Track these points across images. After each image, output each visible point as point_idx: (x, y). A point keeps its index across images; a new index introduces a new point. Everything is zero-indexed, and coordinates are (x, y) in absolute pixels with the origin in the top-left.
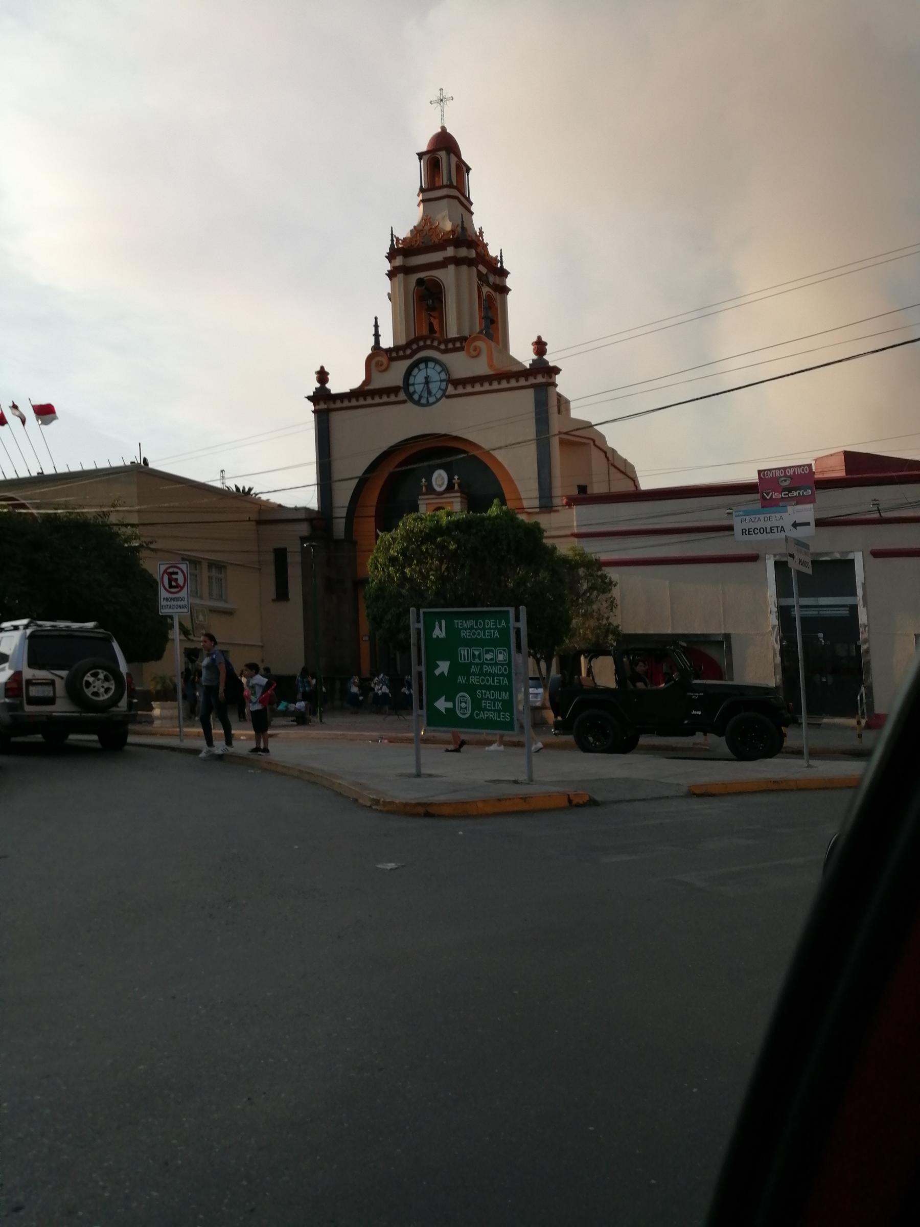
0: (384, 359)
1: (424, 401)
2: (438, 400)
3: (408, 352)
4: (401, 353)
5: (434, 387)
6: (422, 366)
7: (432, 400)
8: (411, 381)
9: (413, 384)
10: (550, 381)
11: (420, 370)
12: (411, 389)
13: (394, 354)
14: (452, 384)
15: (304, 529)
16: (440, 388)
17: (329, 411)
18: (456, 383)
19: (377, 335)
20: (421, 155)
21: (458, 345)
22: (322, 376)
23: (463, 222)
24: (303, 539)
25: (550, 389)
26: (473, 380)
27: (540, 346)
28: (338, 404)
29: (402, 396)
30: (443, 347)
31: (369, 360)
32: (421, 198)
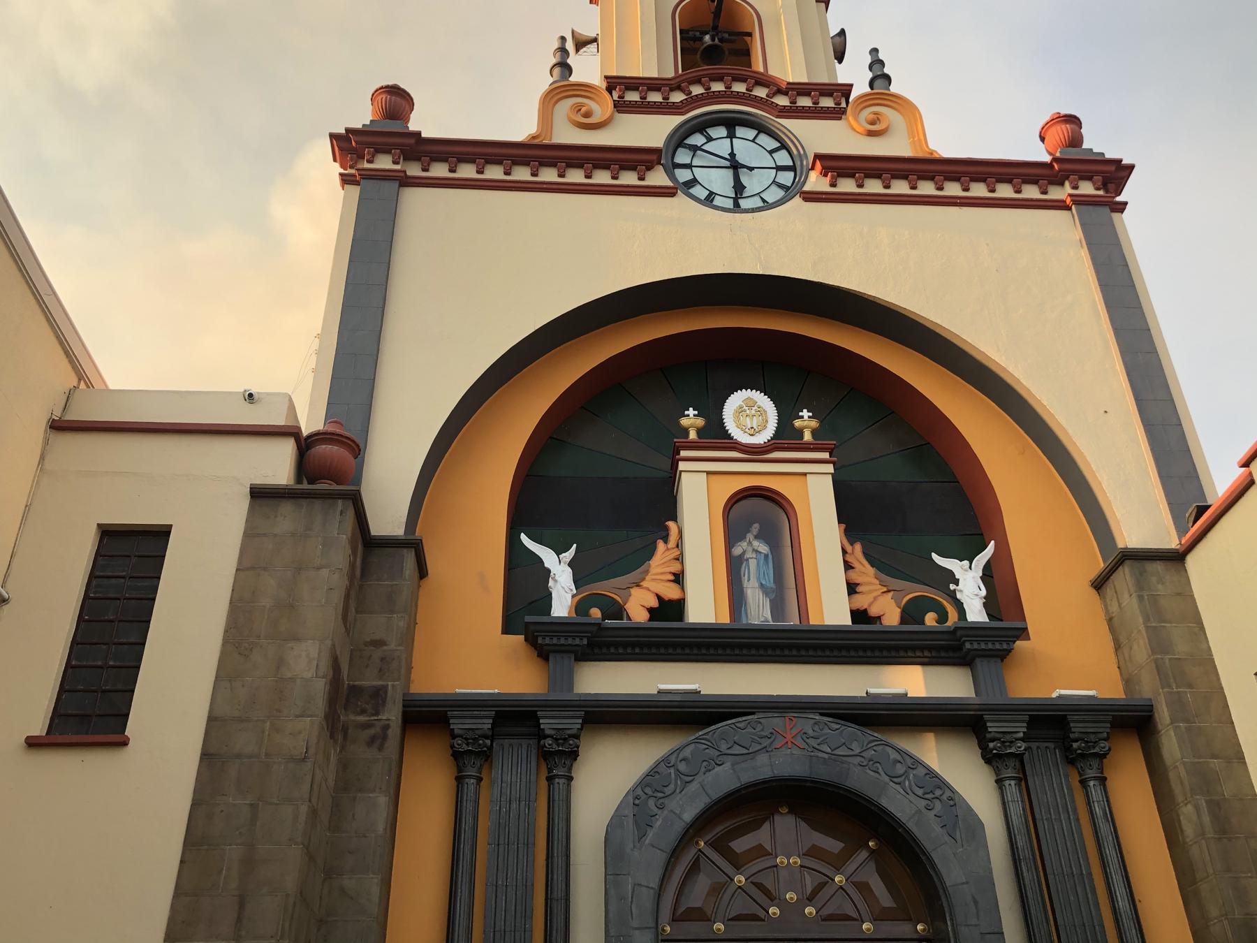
1: (718, 201)
4: (655, 97)
5: (753, 183)
6: (721, 132)
7: (744, 204)
8: (682, 157)
9: (689, 166)
11: (710, 139)
13: (633, 96)
15: (277, 465)
17: (407, 182)
19: (564, 67)
21: (827, 102)
24: (261, 495)
25: (1115, 216)
28: (440, 170)
29: (658, 178)
30: (782, 101)
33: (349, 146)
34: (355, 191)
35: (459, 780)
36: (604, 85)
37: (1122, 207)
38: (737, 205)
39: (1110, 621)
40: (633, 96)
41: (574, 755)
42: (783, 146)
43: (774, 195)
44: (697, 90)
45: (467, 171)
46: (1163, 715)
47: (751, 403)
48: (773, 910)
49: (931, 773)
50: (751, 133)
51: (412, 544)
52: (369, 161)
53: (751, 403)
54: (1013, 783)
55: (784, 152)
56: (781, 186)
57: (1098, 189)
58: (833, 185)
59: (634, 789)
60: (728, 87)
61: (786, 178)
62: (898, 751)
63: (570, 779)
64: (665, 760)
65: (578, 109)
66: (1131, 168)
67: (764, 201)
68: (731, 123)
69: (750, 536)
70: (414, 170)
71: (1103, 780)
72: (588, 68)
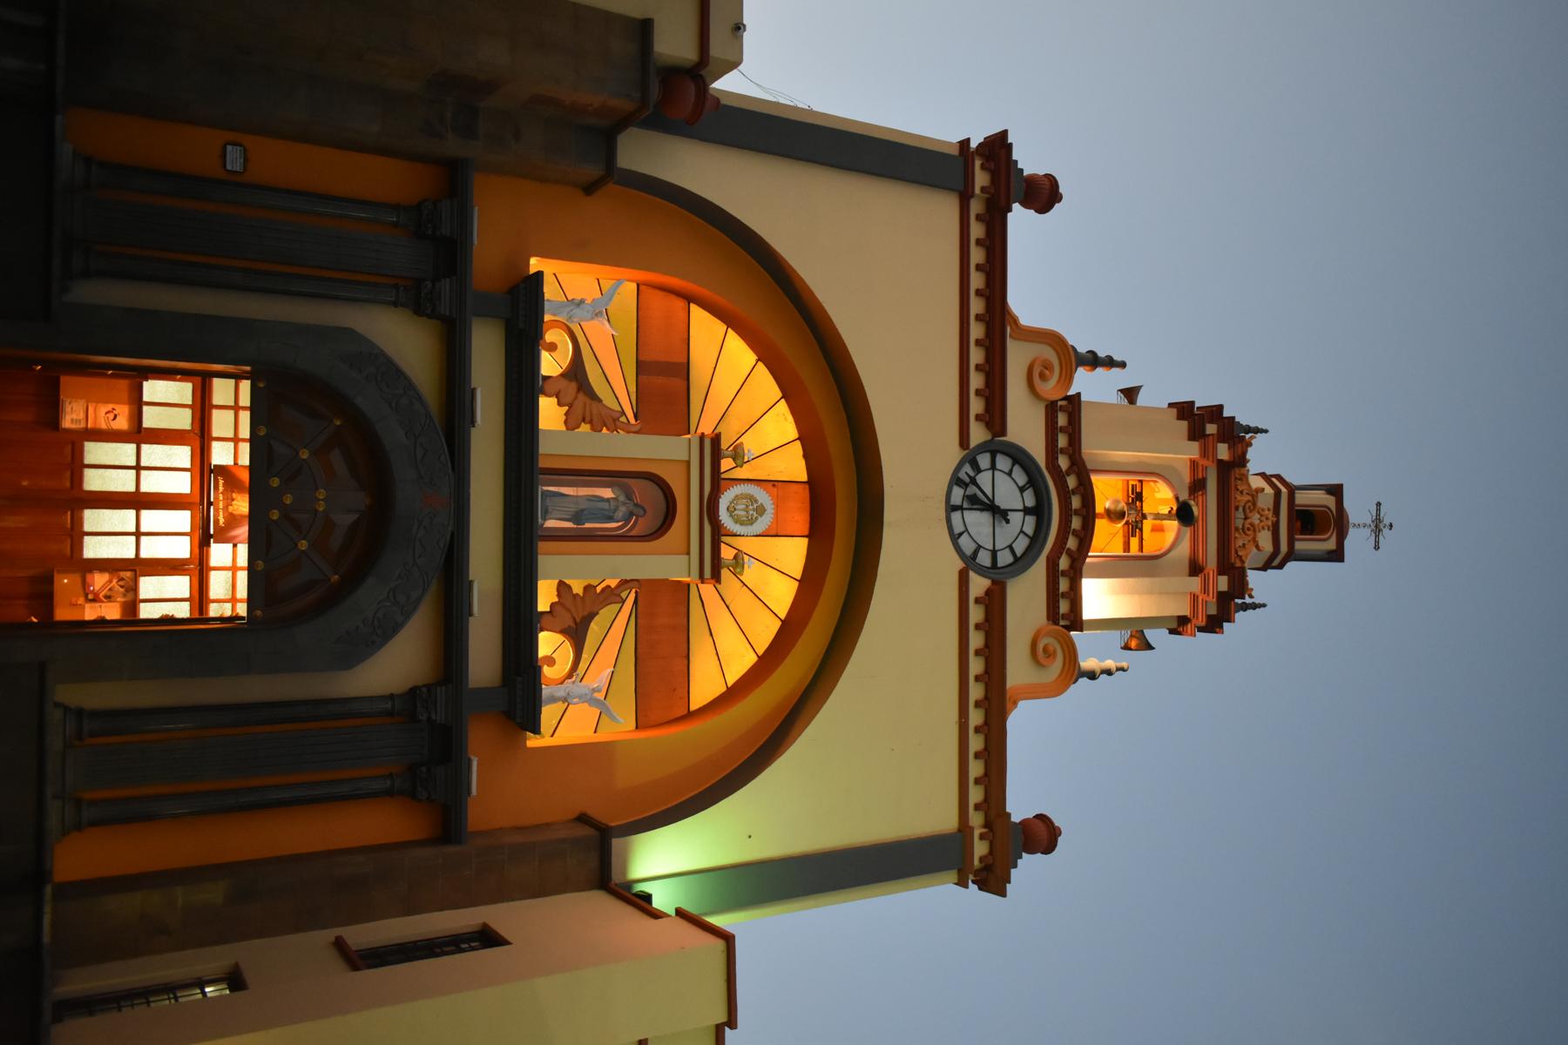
0: (1050, 389)
2: (955, 538)
3: (1063, 462)
4: (1062, 441)
6: (1030, 501)
8: (1003, 462)
9: (993, 467)
10: (971, 877)
11: (1022, 490)
12: (984, 460)
13: (1062, 420)
14: (988, 592)
15: (674, 44)
16: (980, 547)
17: (965, 198)
18: (995, 603)
19: (1093, 361)
20: (1336, 491)
22: (1043, 194)
23: (1255, 606)
24: (644, 29)
26: (995, 651)
27: (1041, 835)
28: (977, 231)
29: (978, 434)
30: (1064, 563)
31: (1054, 340)
32: (1284, 490)
33: (998, 148)
34: (955, 152)
35: (396, 208)
36: (1071, 392)
37: (962, 883)
38: (955, 508)
39: (548, 825)
40: (1062, 420)
41: (418, 311)
42: (1016, 559)
43: (967, 545)
44: (1072, 482)
45: (977, 255)
46: (449, 849)
47: (761, 510)
48: (275, 482)
49: (396, 628)
50: (1029, 529)
51: (607, 176)
52: (983, 167)
53: (761, 510)
54: (389, 706)
55: (1010, 559)
56: (976, 553)
57: (981, 859)
58: (977, 601)
59: (383, 354)
60: (1077, 512)
61: (984, 559)
62: (419, 600)
63: (395, 304)
64: (409, 385)
65: (1047, 366)
66: (1003, 893)
67: (961, 534)
68: (1039, 511)
69: (632, 508)
70: (976, 207)
71: (389, 793)
72: (1090, 386)
